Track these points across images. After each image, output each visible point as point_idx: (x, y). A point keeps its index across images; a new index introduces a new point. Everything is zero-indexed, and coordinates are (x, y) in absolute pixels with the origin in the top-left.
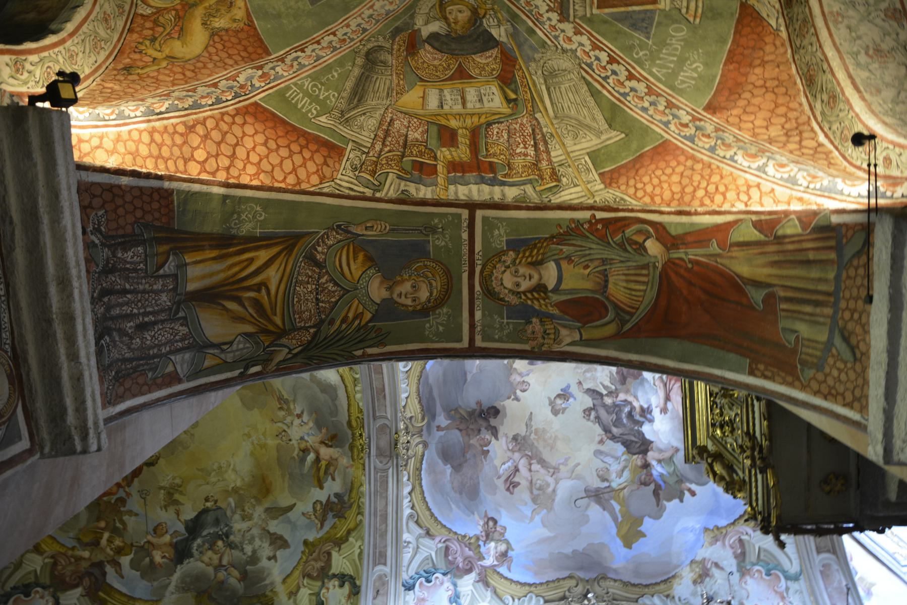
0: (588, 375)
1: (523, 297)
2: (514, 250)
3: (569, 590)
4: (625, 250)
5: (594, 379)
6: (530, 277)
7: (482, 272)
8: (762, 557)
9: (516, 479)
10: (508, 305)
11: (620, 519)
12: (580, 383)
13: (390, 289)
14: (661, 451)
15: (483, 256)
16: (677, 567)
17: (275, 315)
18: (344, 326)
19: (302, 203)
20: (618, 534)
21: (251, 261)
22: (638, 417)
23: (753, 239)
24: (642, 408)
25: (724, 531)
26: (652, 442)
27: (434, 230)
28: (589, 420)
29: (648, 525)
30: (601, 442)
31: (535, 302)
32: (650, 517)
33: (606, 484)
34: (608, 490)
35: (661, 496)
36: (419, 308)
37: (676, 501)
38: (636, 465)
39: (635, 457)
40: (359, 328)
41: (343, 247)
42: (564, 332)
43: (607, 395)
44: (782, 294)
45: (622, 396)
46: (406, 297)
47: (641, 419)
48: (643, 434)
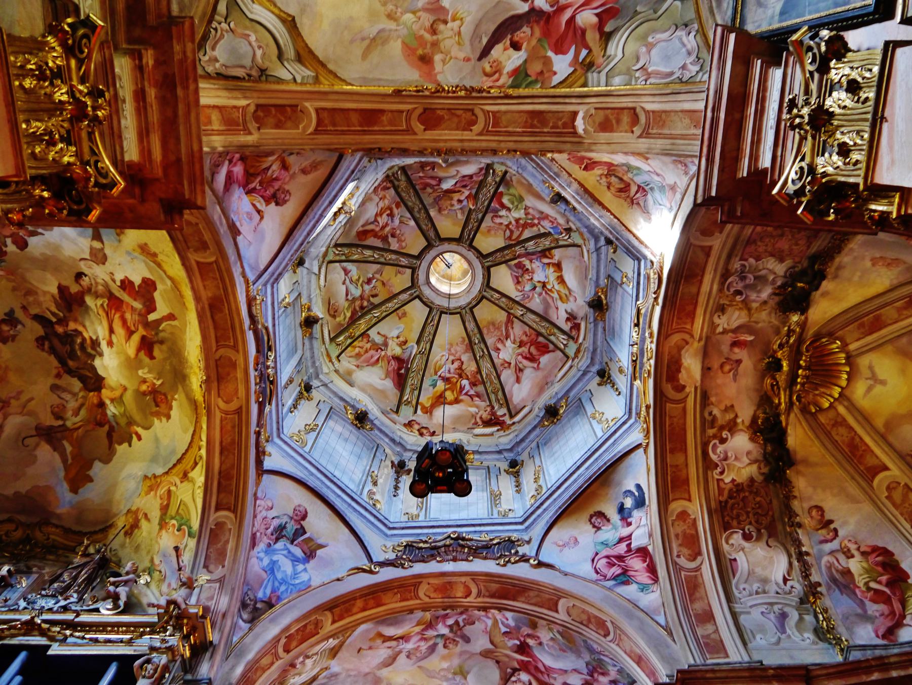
0: (31, 299)
3: (7, 534)
5: (39, 304)
8: (180, 511)
11: (70, 461)
12: (24, 308)
14: (112, 389)
16: (115, 515)
20: (66, 478)
22: (89, 350)
24: (91, 338)
25: (159, 480)
26: (104, 379)
28: (43, 350)
29: (98, 469)
30: (58, 376)
32: (100, 461)
33: (60, 423)
34: (61, 429)
35: (114, 439)
37: (126, 445)
38: (93, 403)
39: (91, 394)
43: (56, 323)
45: (72, 326)
47: (93, 352)
48: (95, 369)
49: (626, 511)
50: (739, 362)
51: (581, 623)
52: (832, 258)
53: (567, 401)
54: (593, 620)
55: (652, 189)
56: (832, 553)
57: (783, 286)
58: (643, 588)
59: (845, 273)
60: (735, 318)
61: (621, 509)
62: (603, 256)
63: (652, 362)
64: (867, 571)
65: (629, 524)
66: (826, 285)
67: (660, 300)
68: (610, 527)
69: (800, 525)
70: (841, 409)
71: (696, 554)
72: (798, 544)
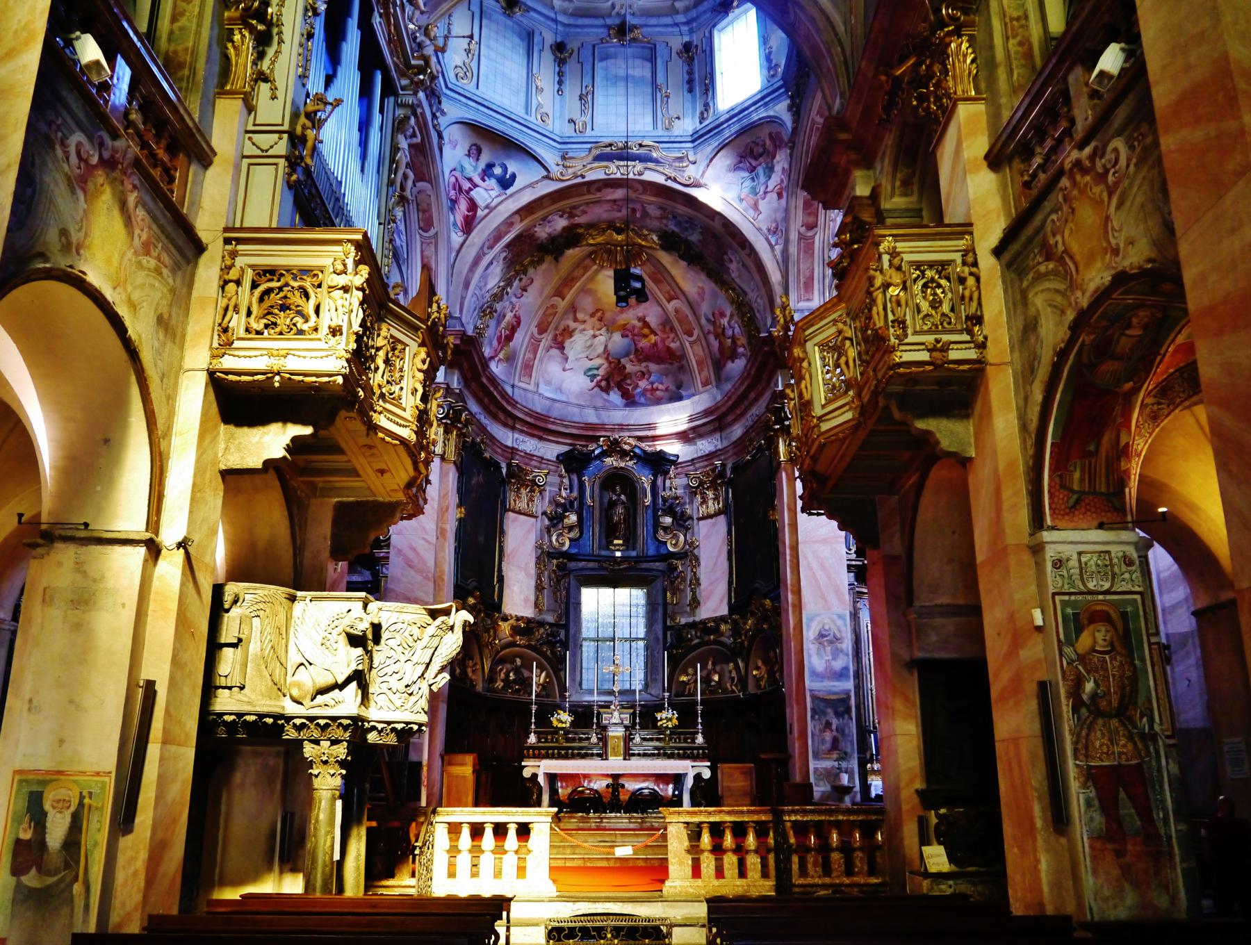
49: (490, 172)
50: (620, 211)
51: (418, 205)
52: (703, 270)
53: (525, 11)
54: (427, 215)
55: (753, 179)
56: (511, 302)
57: (680, 237)
58: (455, 224)
59: (692, 273)
60: (653, 211)
61: (490, 166)
62: (670, 29)
63: (618, 175)
64: (508, 324)
65: (484, 181)
66: (684, 264)
67: (670, 183)
68: (474, 164)
69: (521, 280)
70: (595, 267)
71: (491, 247)
72: (509, 283)
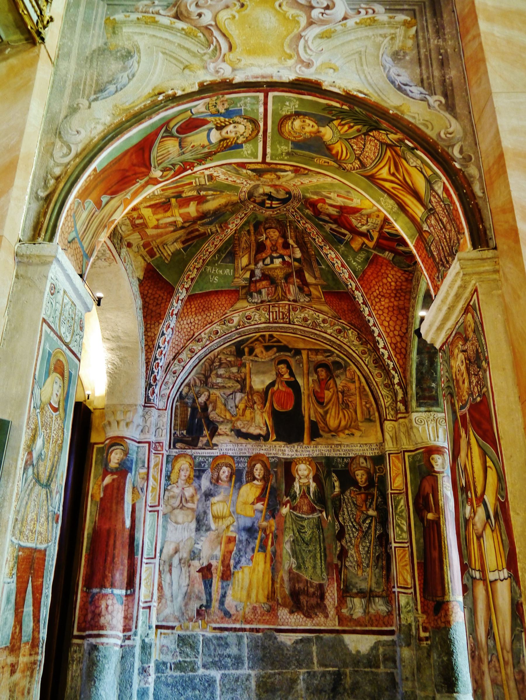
1: (231, 122)
2: (238, 144)
4: (172, 165)
6: (227, 133)
7: (259, 132)
9: (231, 17)
10: (241, 116)
13: (319, 132)
15: (257, 140)
17: (389, 157)
18: (352, 124)
19: (361, 189)
21: (393, 188)
23: (114, 216)
27: (288, 154)
31: (223, 120)
36: (301, 117)
40: (343, 119)
41: (344, 160)
42: (203, 109)
44: (96, 213)
46: (309, 125)
